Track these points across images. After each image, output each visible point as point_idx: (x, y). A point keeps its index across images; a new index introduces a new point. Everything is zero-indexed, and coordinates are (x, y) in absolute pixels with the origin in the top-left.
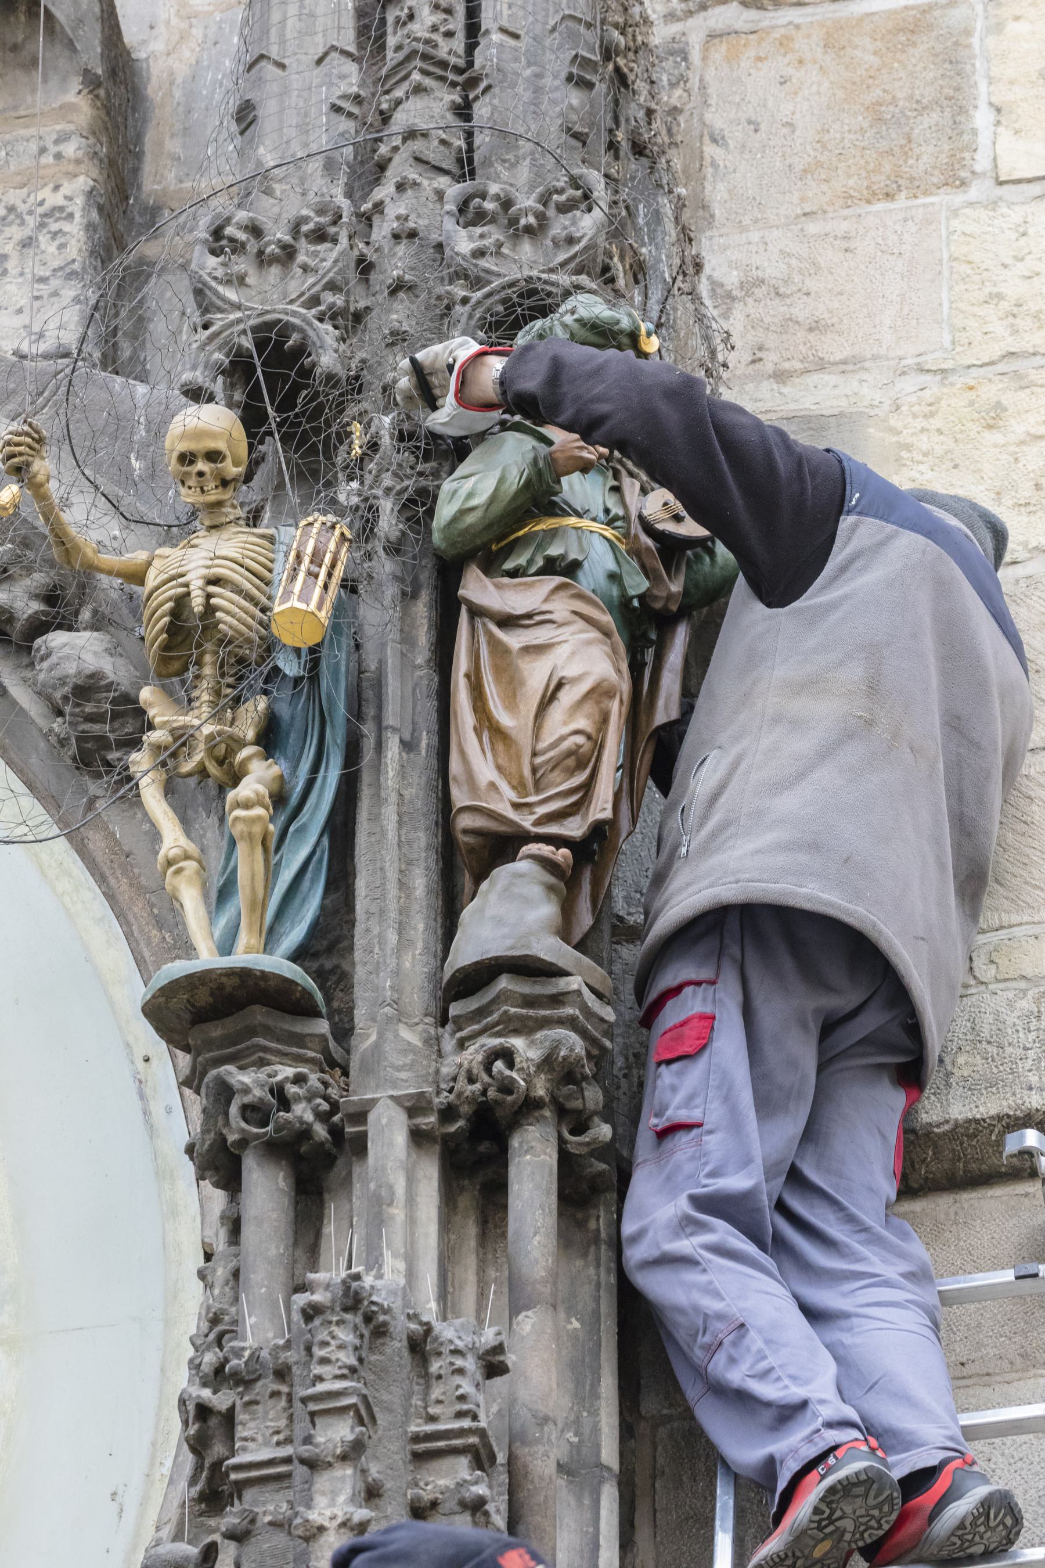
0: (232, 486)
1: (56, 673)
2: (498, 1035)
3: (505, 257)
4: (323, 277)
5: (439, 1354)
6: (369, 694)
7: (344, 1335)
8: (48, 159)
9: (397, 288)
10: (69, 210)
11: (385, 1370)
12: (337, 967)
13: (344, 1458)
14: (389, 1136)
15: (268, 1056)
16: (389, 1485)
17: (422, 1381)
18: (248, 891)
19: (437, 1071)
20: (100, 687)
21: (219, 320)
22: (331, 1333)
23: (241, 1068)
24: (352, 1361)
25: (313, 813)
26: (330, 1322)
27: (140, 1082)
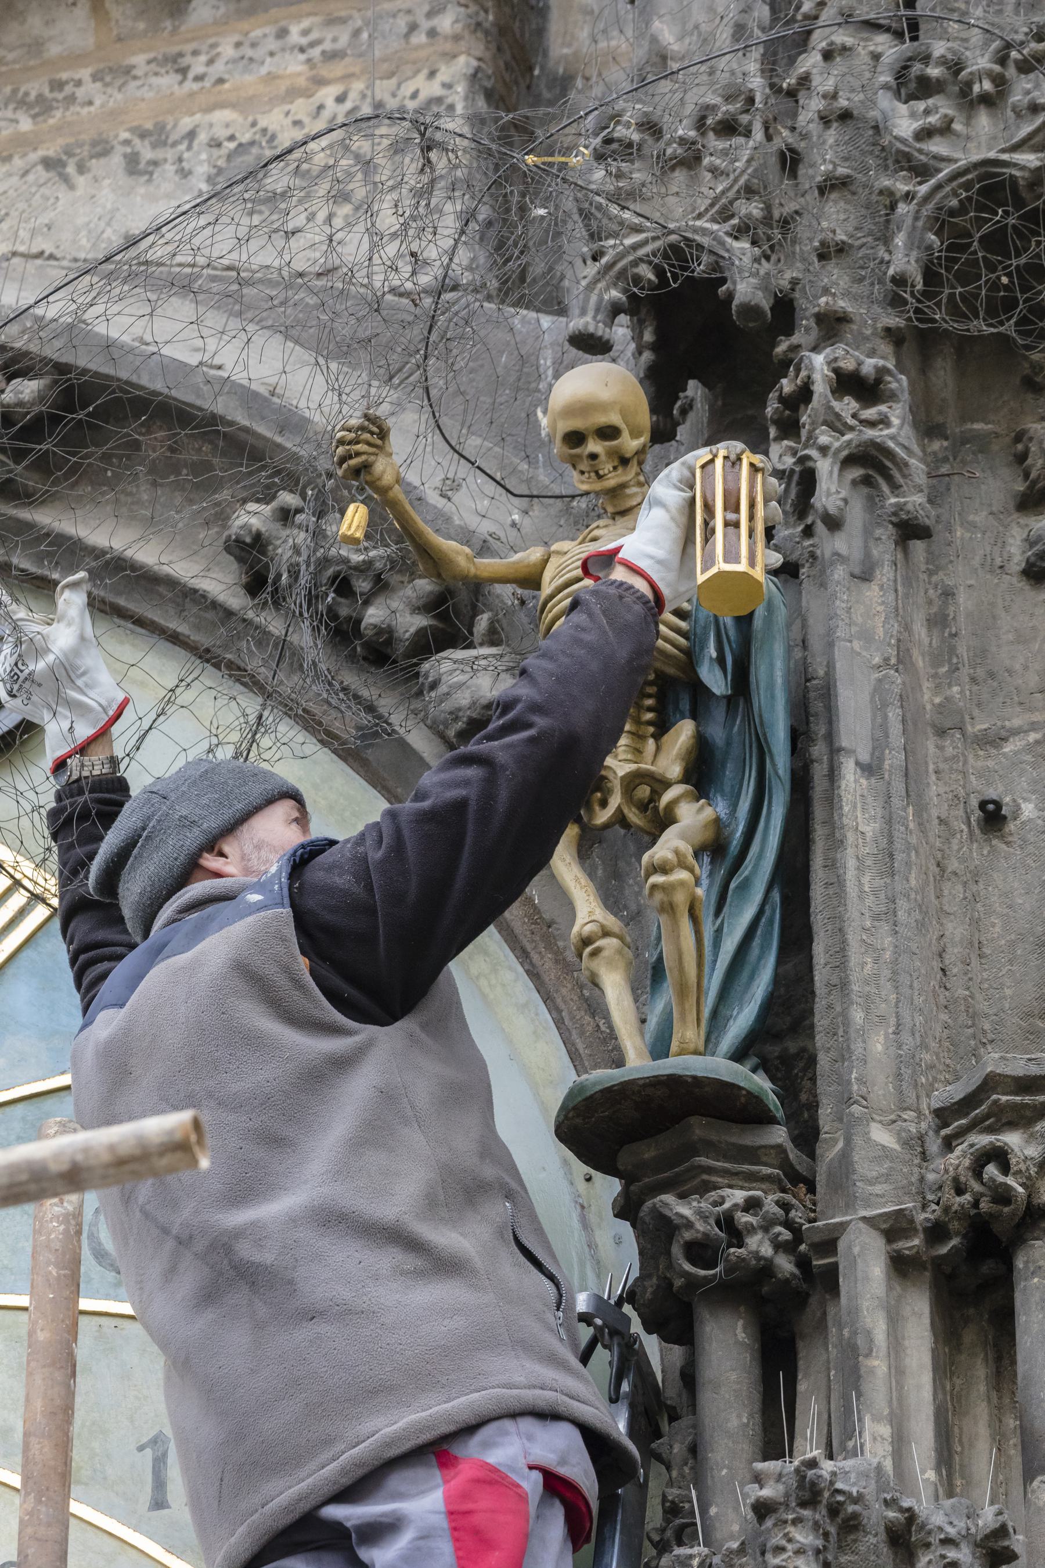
0: (635, 461)
2: (991, 1130)
3: (958, 135)
4: (736, 180)
5: (928, 1545)
7: (803, 1537)
8: (420, 38)
9: (831, 186)
10: (449, 101)
12: (804, 1050)
14: (866, 1269)
15: (714, 1179)
18: (676, 973)
19: (922, 1179)
22: (786, 1535)
23: (682, 1196)
25: (756, 866)
26: (786, 1522)
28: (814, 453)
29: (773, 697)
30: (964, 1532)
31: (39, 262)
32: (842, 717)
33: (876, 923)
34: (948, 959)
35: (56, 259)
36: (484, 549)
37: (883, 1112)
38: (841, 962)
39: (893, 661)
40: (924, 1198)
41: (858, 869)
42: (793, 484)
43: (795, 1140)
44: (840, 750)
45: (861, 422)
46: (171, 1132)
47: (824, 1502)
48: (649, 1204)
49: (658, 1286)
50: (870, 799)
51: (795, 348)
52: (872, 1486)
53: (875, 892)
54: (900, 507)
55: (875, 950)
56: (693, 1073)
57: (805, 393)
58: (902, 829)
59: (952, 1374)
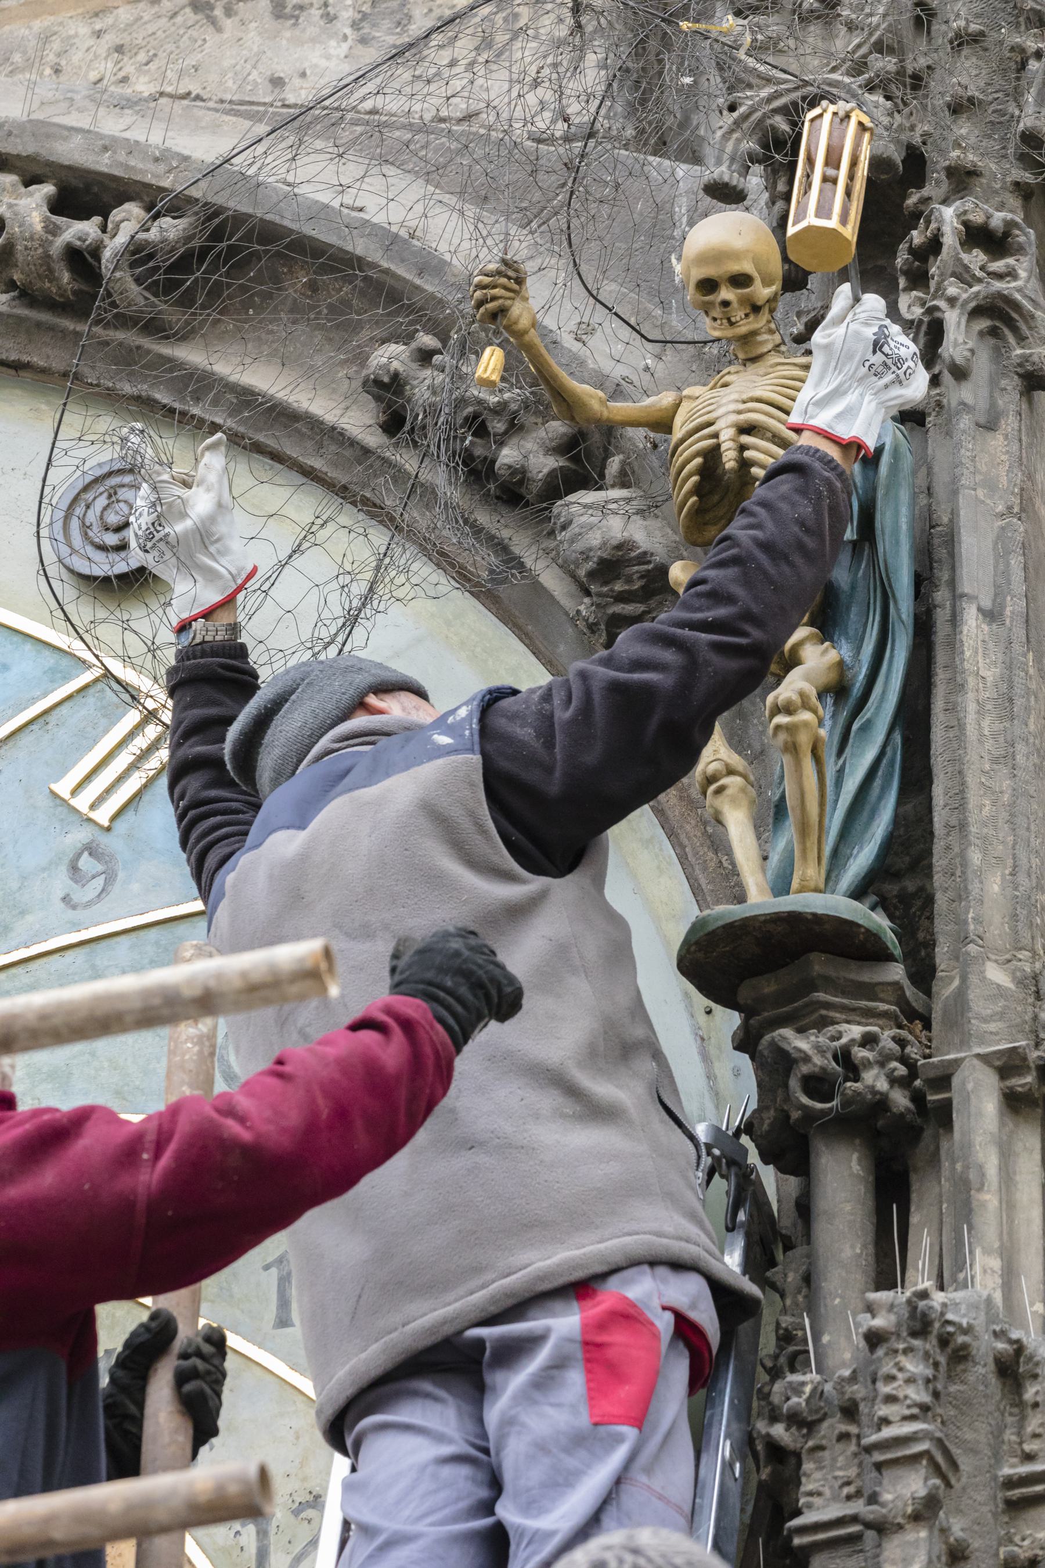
0: (766, 310)
1: (579, 546)
4: (871, 34)
6: (941, 553)
7: (914, 1366)
9: (963, 41)
11: (968, 1403)
12: (922, 889)
13: (916, 1518)
15: (832, 1014)
16: (976, 1544)
17: (1016, 1410)
19: (1035, 1018)
20: (630, 560)
21: (750, 98)
22: (897, 1364)
23: (801, 1030)
24: (925, 1398)
25: (878, 708)
26: (896, 1351)
27: (703, 1039)
28: (942, 304)
29: (897, 542)
31: (185, 102)
32: (964, 563)
33: (995, 766)
35: (204, 101)
36: (617, 392)
37: (998, 951)
38: (960, 805)
39: (1016, 510)
40: (1037, 1036)
41: (978, 712)
42: (922, 334)
43: (913, 977)
44: (963, 595)
45: (989, 274)
46: (301, 960)
47: (935, 1332)
48: (767, 1038)
49: (775, 1118)
50: (991, 645)
51: (927, 200)
52: (982, 1317)
53: (994, 736)
54: (1026, 358)
55: (994, 793)
56: (813, 910)
57: (934, 245)
58: (1022, 674)
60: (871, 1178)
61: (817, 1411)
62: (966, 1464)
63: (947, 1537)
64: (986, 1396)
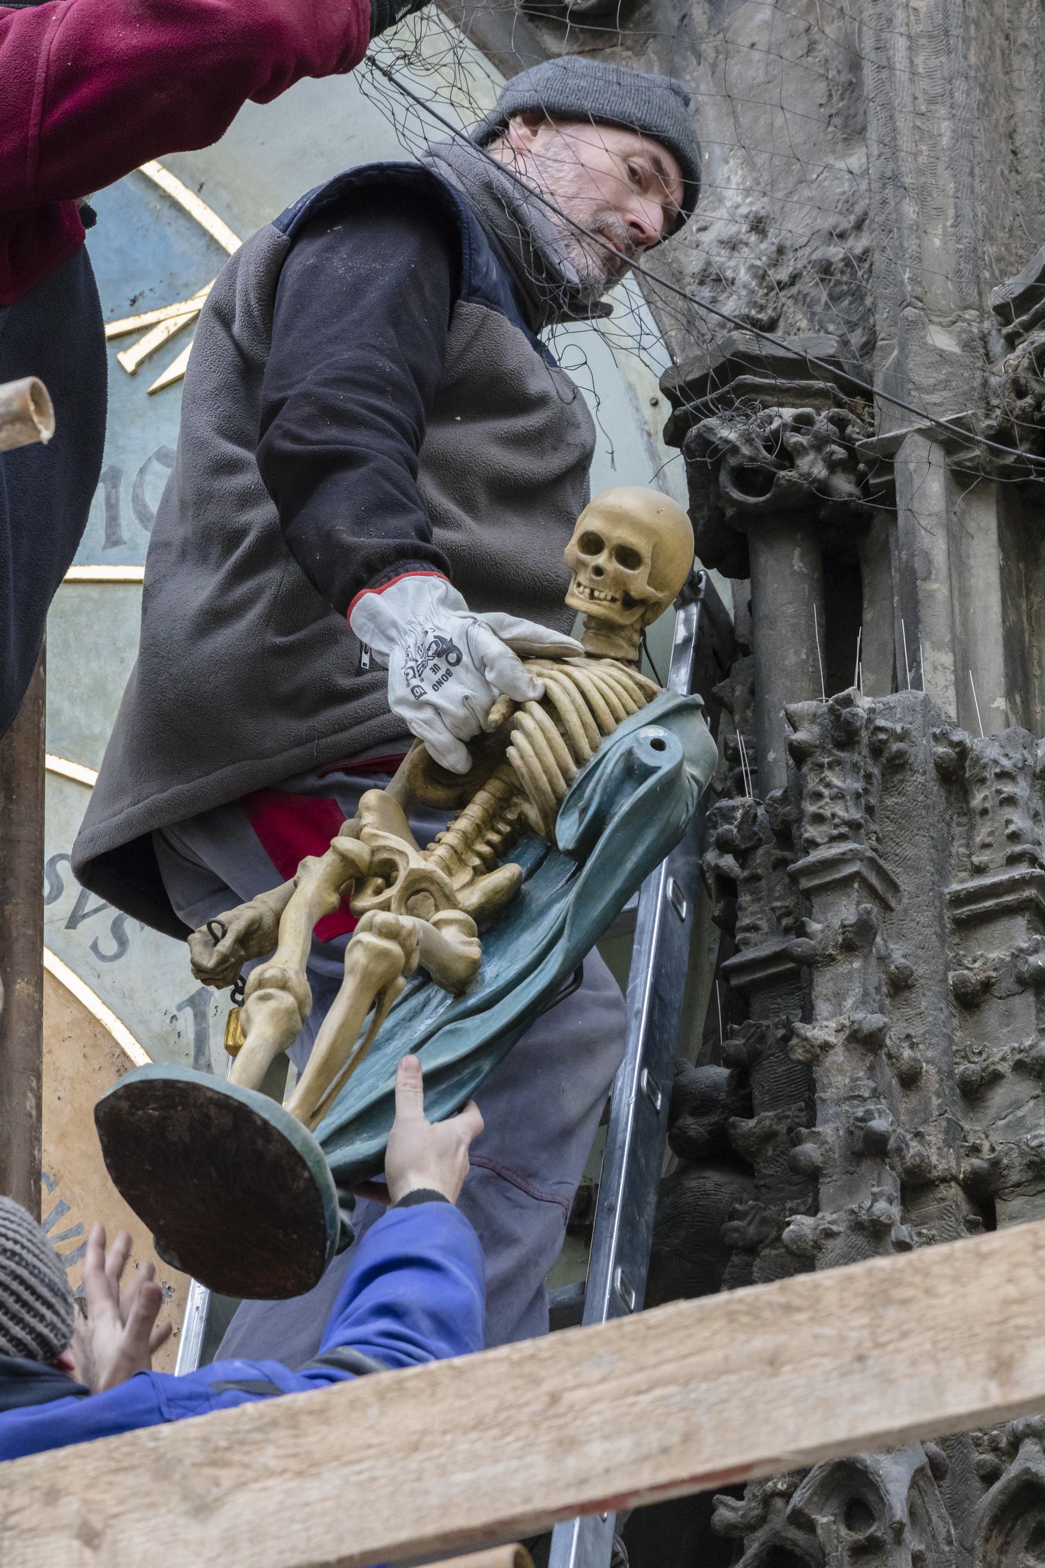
5: (983, 781)
11: (906, 816)
14: (925, 484)
16: (920, 970)
17: (964, 820)
19: (985, 383)
26: (821, 766)
27: (649, 435)
30: (1020, 765)
33: (932, 107)
34: (1020, 139)
37: (943, 314)
40: (988, 403)
41: (910, 48)
48: (693, 431)
55: (931, 136)
59: (1029, 591)
60: (816, 575)
61: (750, 838)
62: (906, 882)
63: (887, 966)
64: (927, 807)
